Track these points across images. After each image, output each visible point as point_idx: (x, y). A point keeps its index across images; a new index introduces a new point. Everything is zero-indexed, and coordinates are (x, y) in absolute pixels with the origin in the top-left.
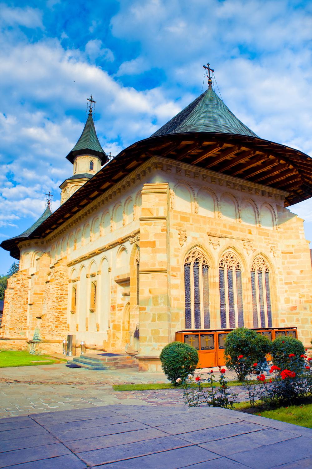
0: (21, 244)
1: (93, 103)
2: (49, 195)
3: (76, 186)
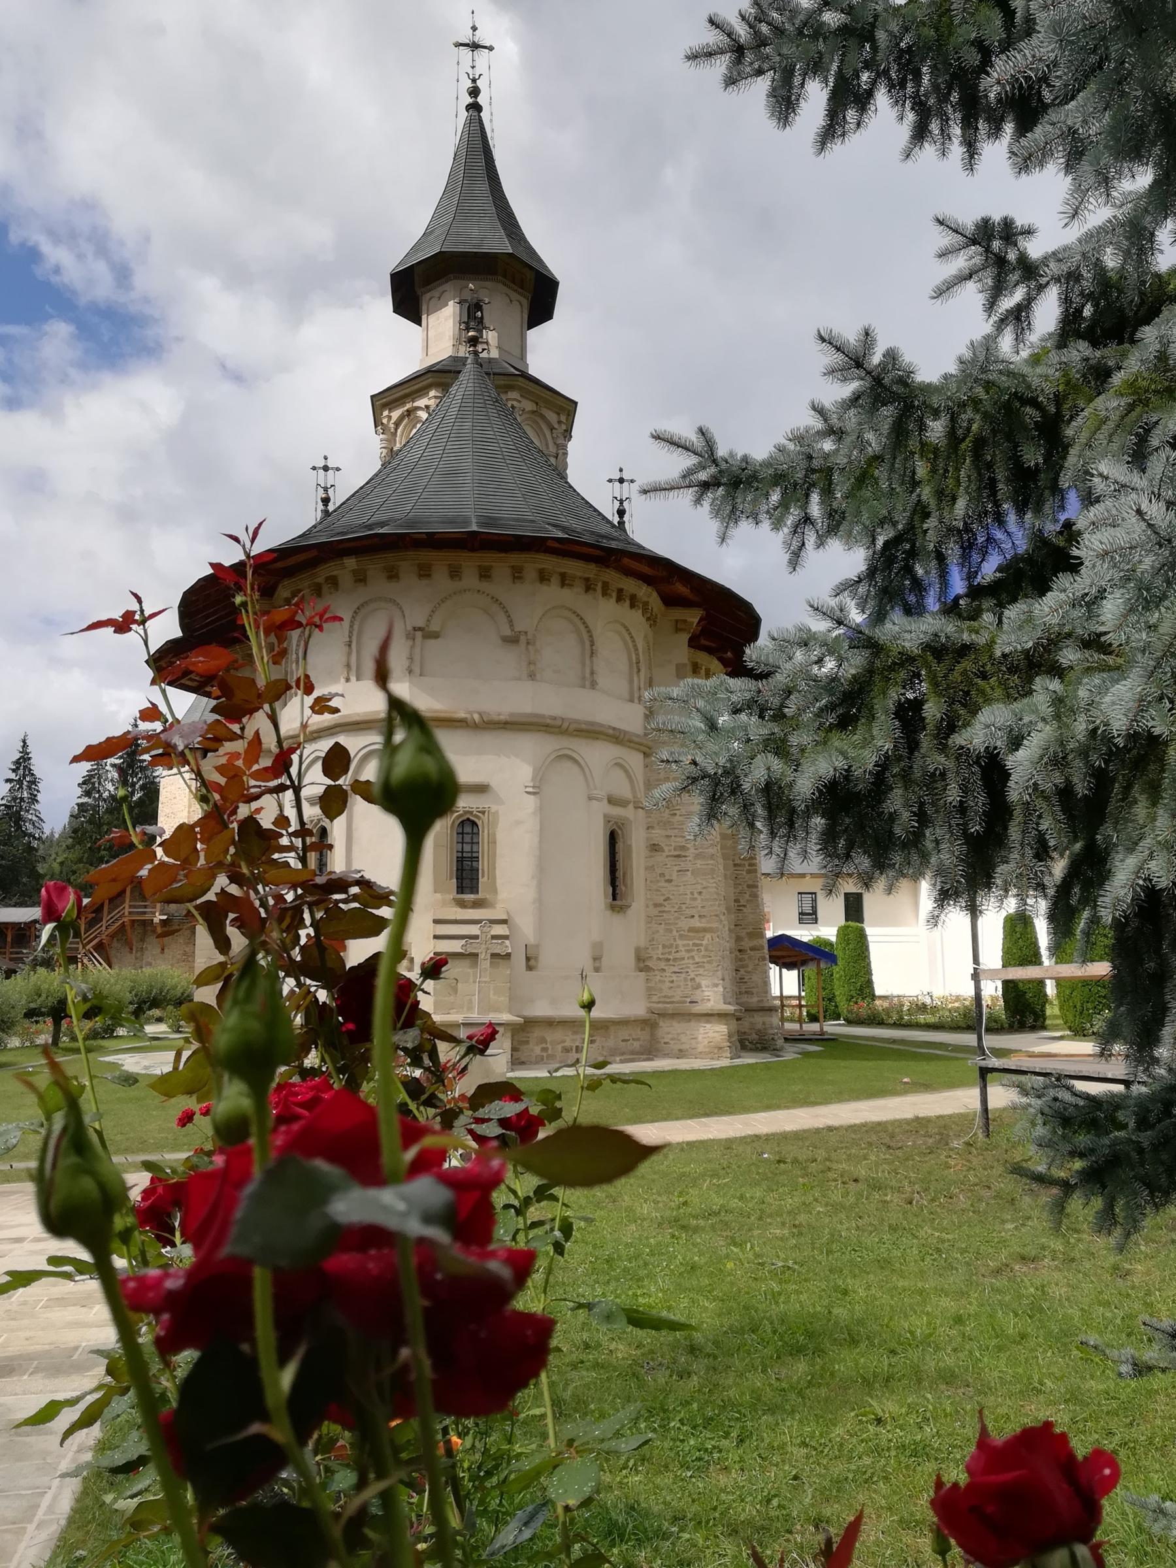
1: (482, 56)
2: (326, 468)
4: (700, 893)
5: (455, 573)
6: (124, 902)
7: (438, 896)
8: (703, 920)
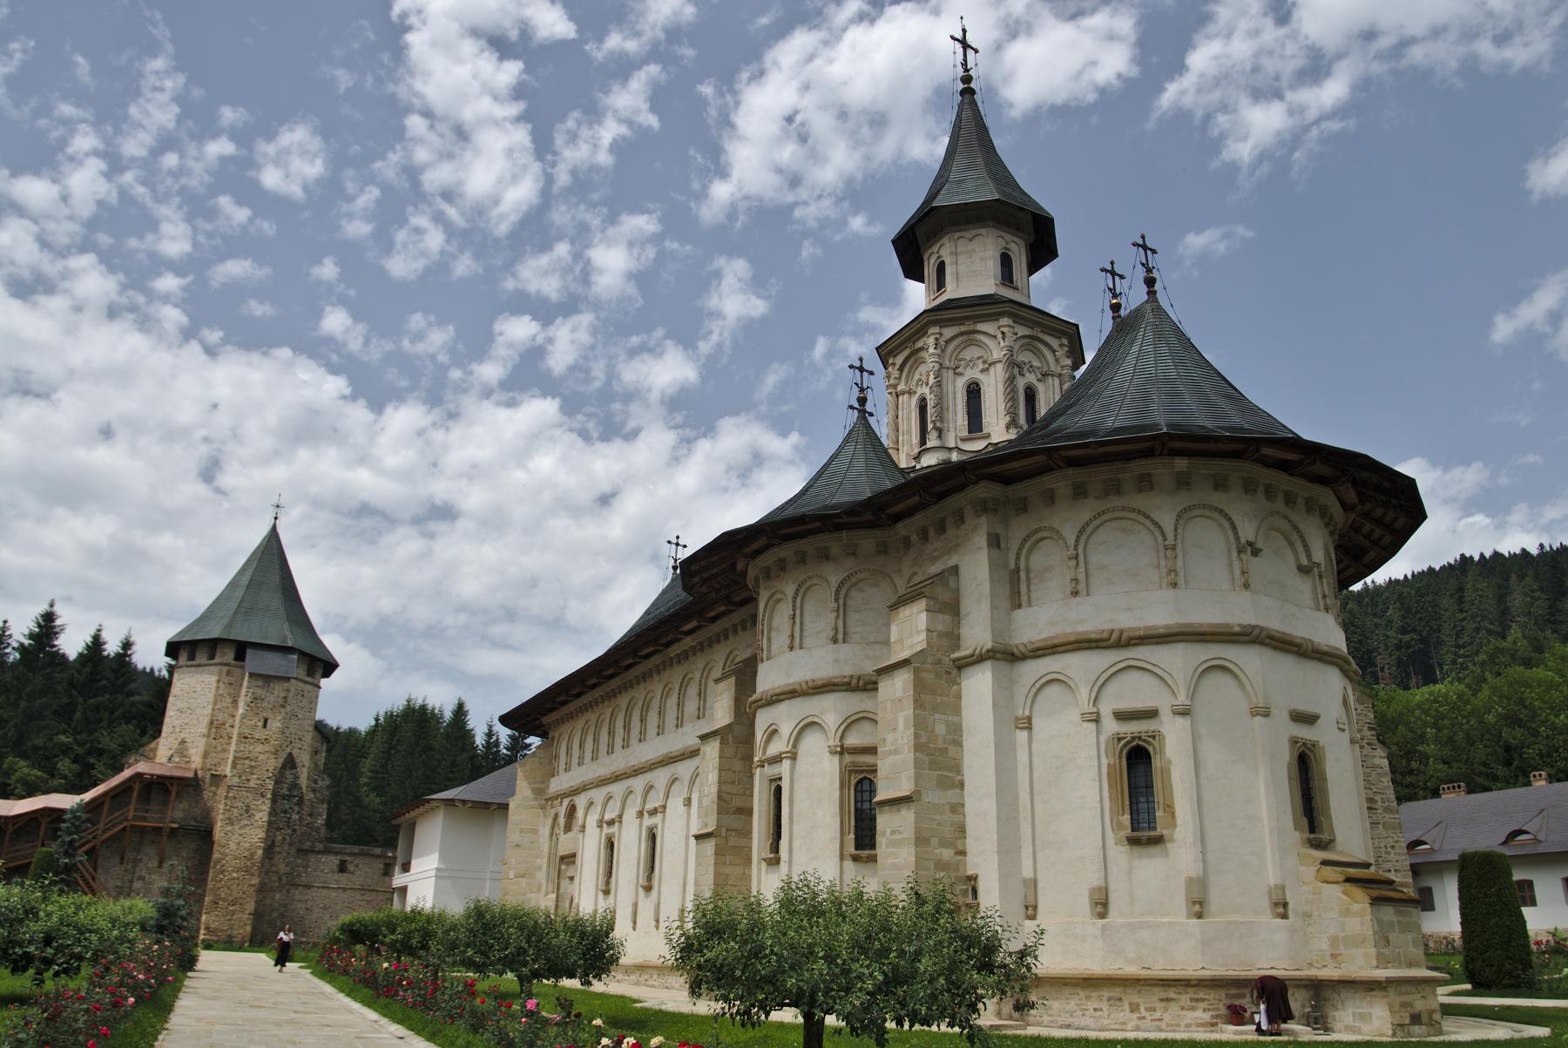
0: (782, 555)
3: (964, 338)
4: (1393, 847)
5: (1270, 493)
6: (128, 804)
7: (1297, 833)
8: (1399, 875)
